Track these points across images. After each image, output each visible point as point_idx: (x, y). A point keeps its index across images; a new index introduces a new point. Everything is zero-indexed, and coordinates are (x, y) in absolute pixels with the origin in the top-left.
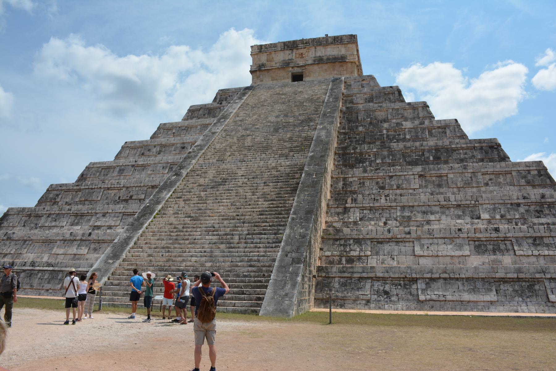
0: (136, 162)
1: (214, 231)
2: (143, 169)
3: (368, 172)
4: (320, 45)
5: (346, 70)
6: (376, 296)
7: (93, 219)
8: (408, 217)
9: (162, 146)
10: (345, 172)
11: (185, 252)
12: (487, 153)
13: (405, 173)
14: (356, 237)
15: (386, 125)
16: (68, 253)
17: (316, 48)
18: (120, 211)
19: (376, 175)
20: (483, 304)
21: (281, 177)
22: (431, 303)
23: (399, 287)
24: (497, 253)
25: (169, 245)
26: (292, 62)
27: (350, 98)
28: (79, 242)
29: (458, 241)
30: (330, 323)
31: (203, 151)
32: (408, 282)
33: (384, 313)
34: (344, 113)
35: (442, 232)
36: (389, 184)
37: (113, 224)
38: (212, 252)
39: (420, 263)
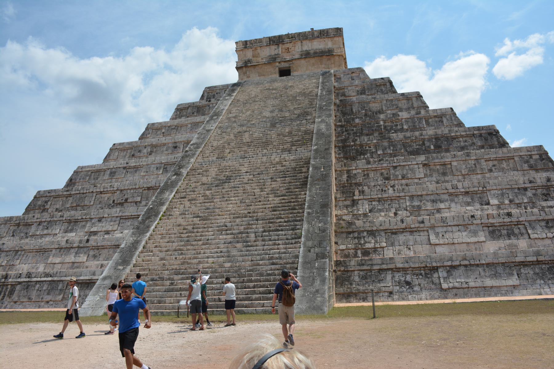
0: (127, 163)
1: (227, 230)
2: (136, 171)
3: (372, 163)
4: (306, 39)
5: (334, 63)
6: (398, 288)
7: (88, 225)
8: (418, 206)
9: (153, 146)
10: (348, 165)
11: (200, 253)
12: (486, 139)
13: (409, 163)
14: (370, 229)
15: (382, 116)
16: (66, 261)
17: (302, 42)
18: (117, 215)
19: (380, 166)
20: (506, 289)
21: (288, 171)
22: (455, 290)
23: (421, 277)
24: (512, 237)
25: (182, 247)
26: (279, 57)
27: (341, 91)
28: (77, 249)
29: (472, 227)
30: (374, 317)
31: (201, 149)
32: (429, 271)
33: (411, 304)
34: (338, 106)
35: (455, 220)
36: (394, 175)
37: (110, 229)
38: (228, 252)
39: (437, 251)
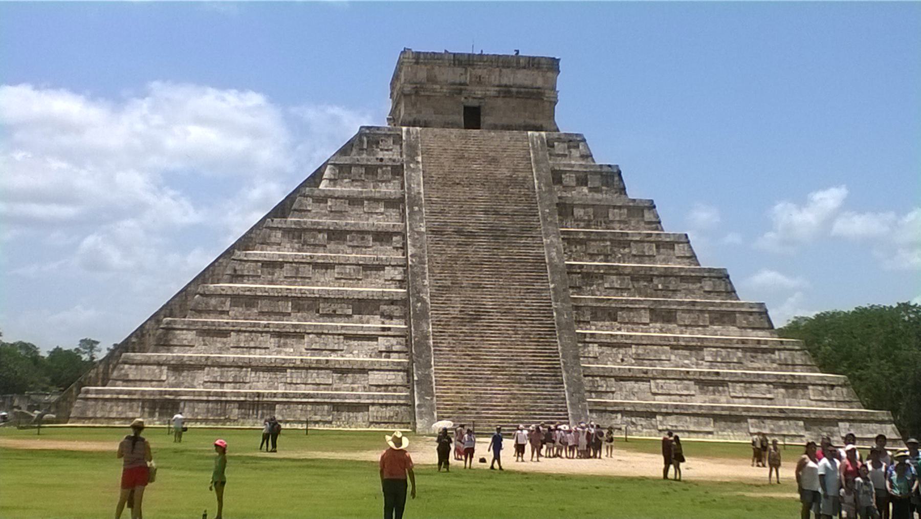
17: (501, 71)
18: (339, 332)
29: (686, 382)
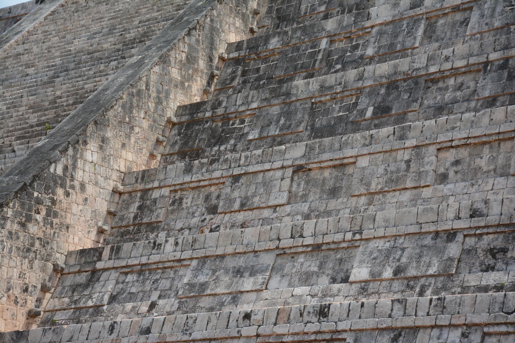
13: (267, 166)
